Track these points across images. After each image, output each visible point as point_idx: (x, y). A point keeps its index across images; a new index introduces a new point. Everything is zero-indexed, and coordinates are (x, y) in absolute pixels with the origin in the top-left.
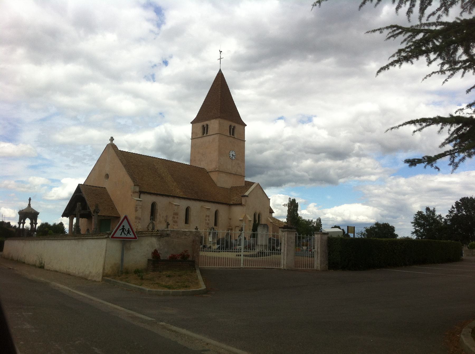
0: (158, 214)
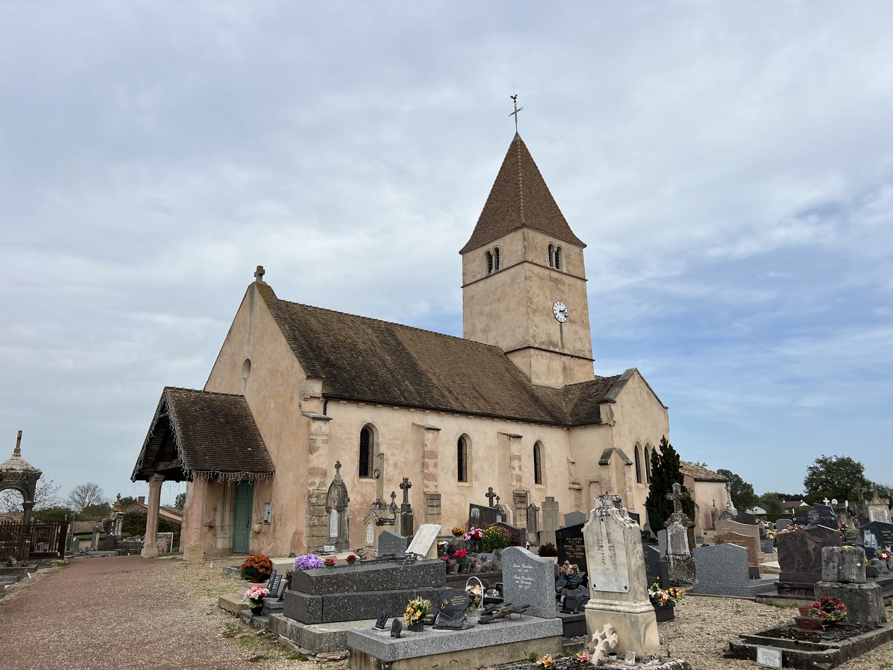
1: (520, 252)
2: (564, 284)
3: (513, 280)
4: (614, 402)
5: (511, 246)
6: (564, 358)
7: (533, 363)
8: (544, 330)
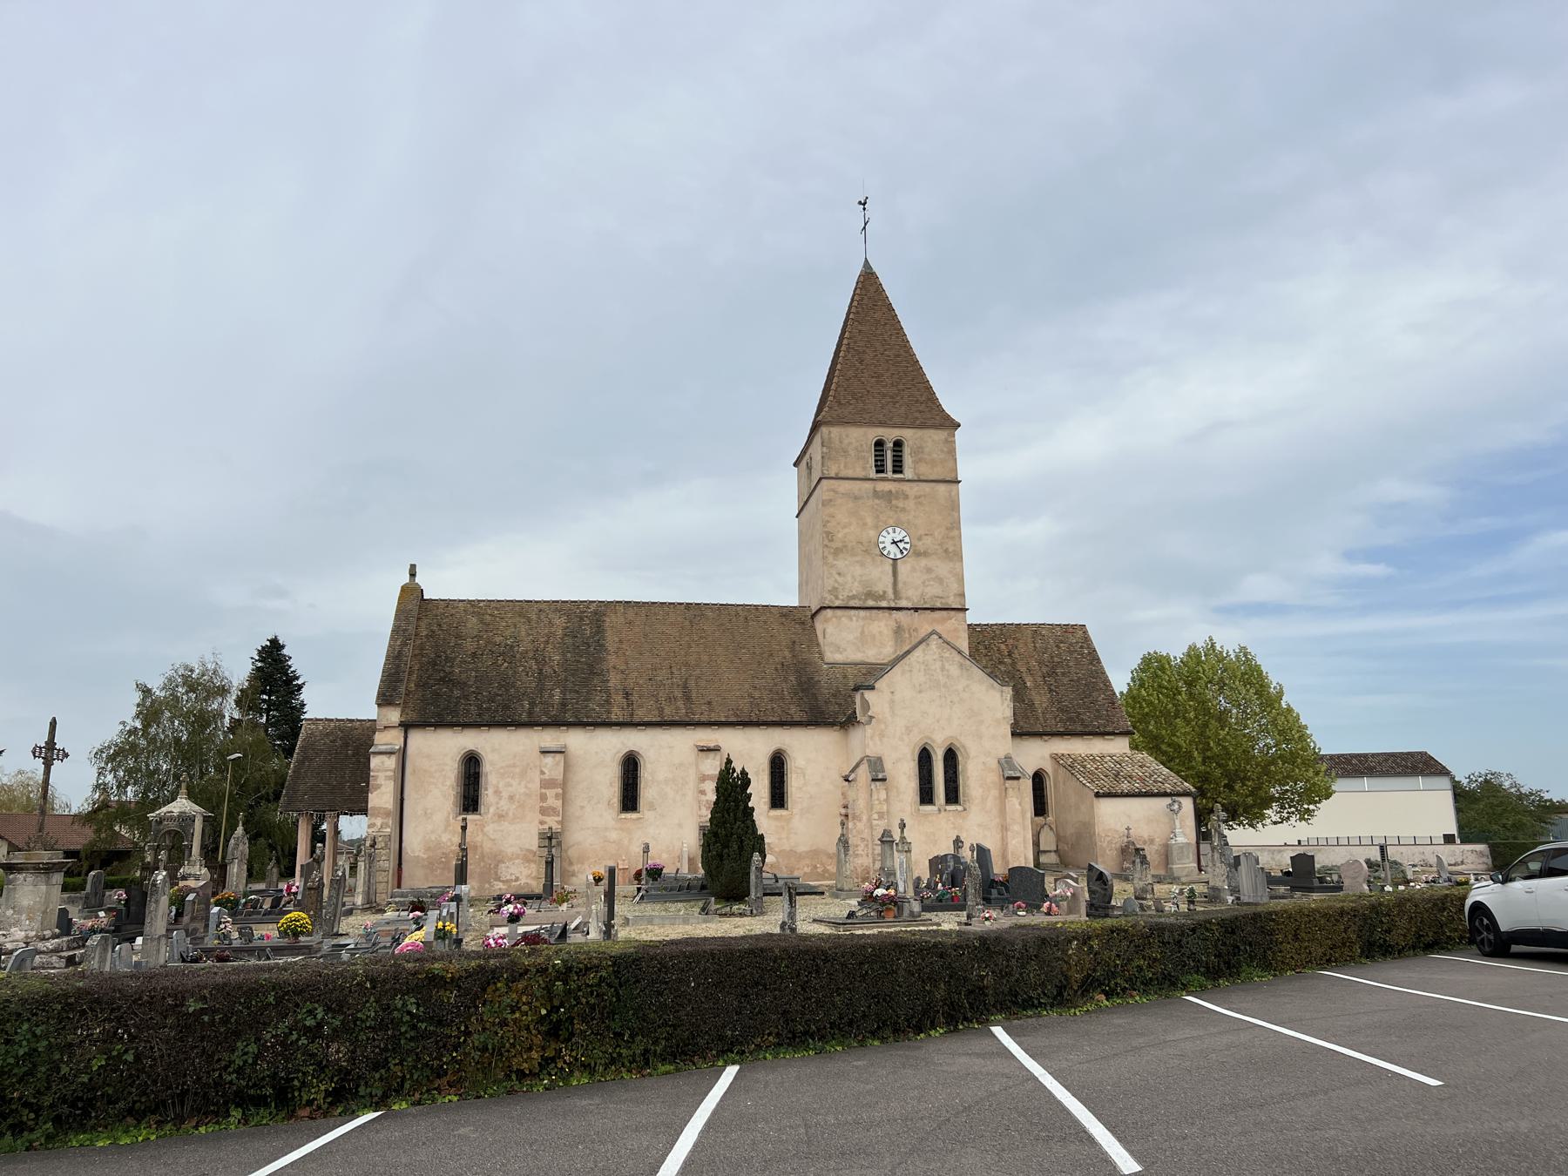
2: (906, 497)
4: (872, 688)
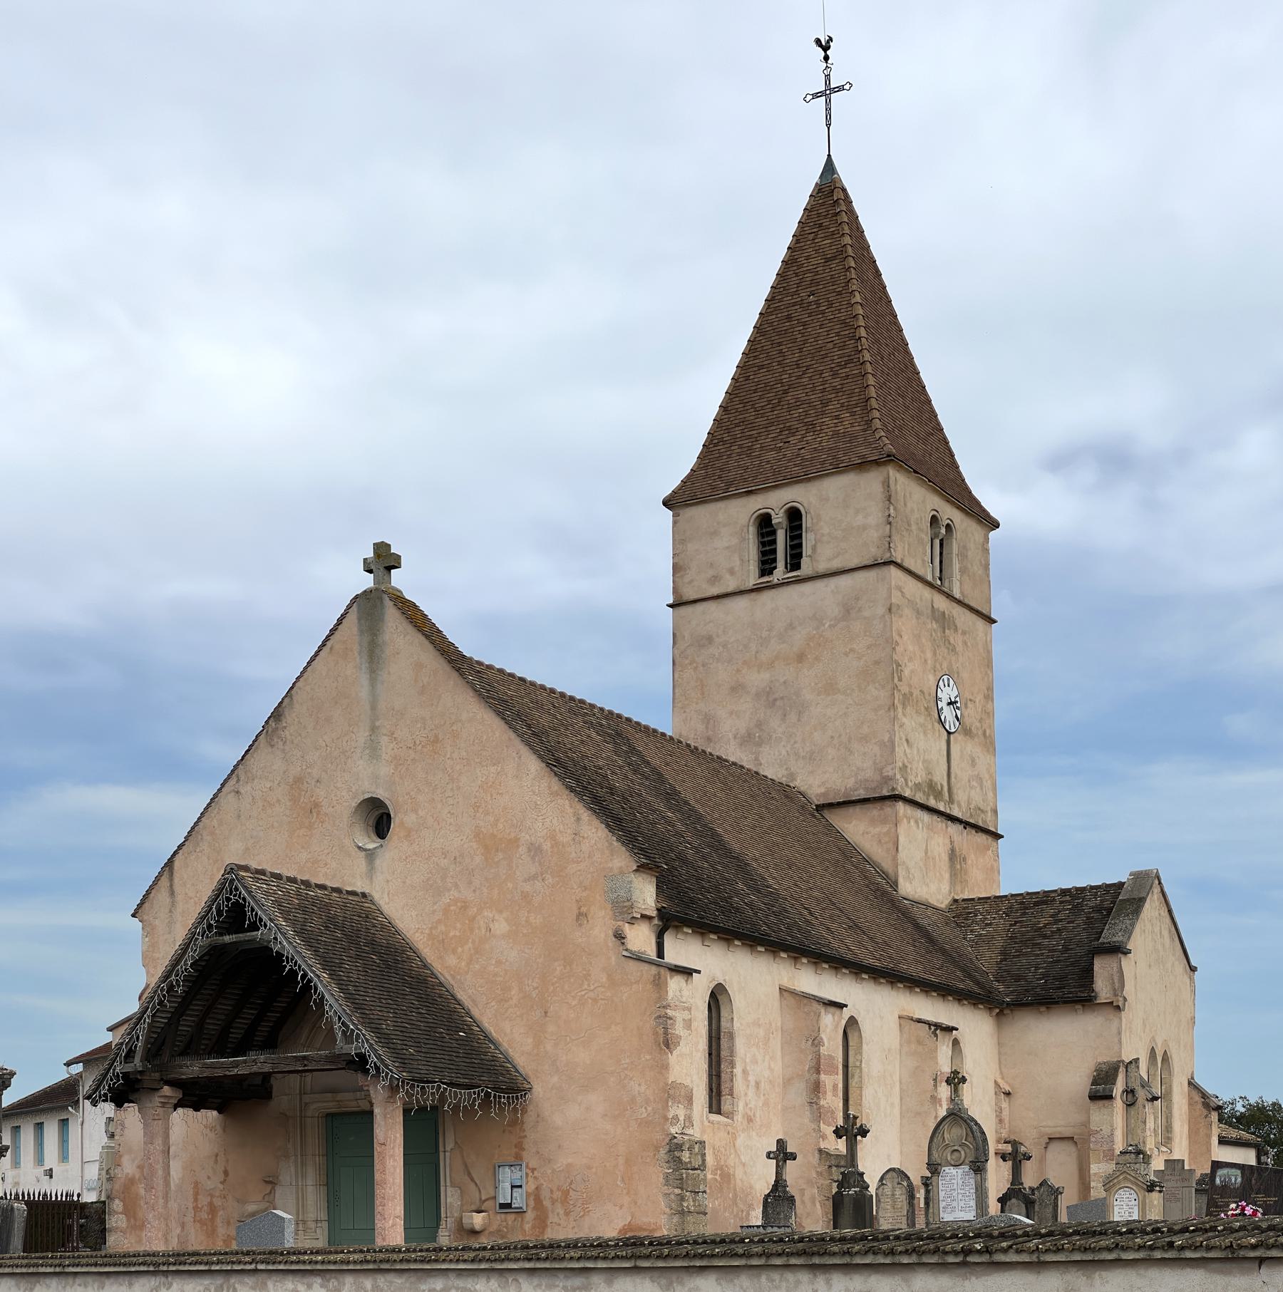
0: (738, 1071)
1: (874, 535)
2: (956, 629)
3: (848, 610)
5: (843, 510)
6: (954, 829)
7: (901, 839)
8: (919, 755)
